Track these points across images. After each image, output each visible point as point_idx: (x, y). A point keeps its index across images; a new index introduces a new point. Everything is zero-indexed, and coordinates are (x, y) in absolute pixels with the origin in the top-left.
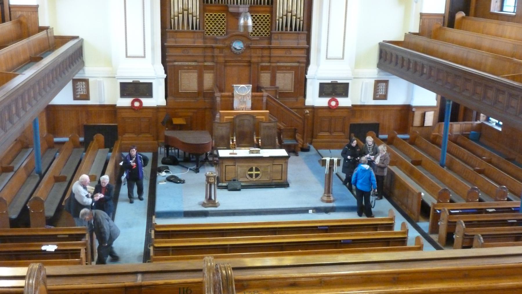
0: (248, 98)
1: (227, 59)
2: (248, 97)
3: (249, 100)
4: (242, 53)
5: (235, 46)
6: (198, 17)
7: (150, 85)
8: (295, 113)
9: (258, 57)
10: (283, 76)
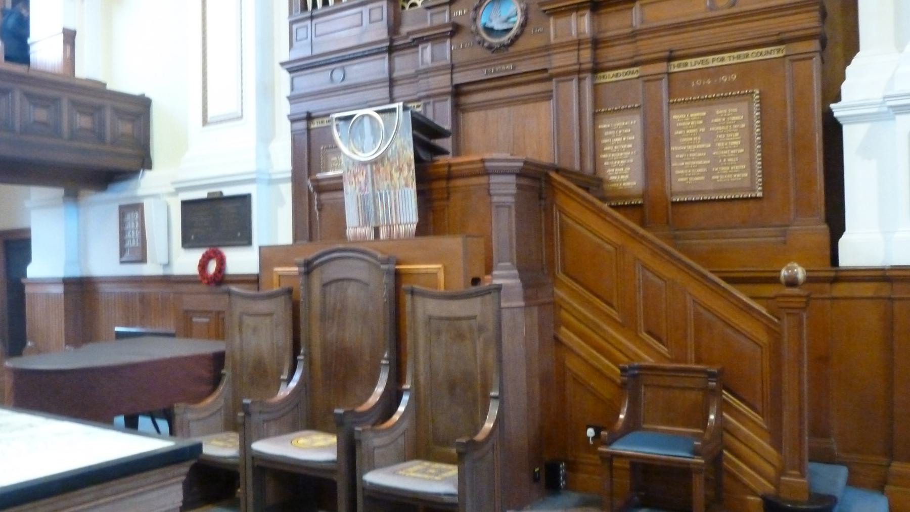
0: (396, 175)
1: (459, 78)
2: (400, 170)
3: (406, 189)
4: (513, 41)
5: (491, 21)
7: (244, 200)
8: (723, 284)
9: (579, 43)
10: (702, 118)
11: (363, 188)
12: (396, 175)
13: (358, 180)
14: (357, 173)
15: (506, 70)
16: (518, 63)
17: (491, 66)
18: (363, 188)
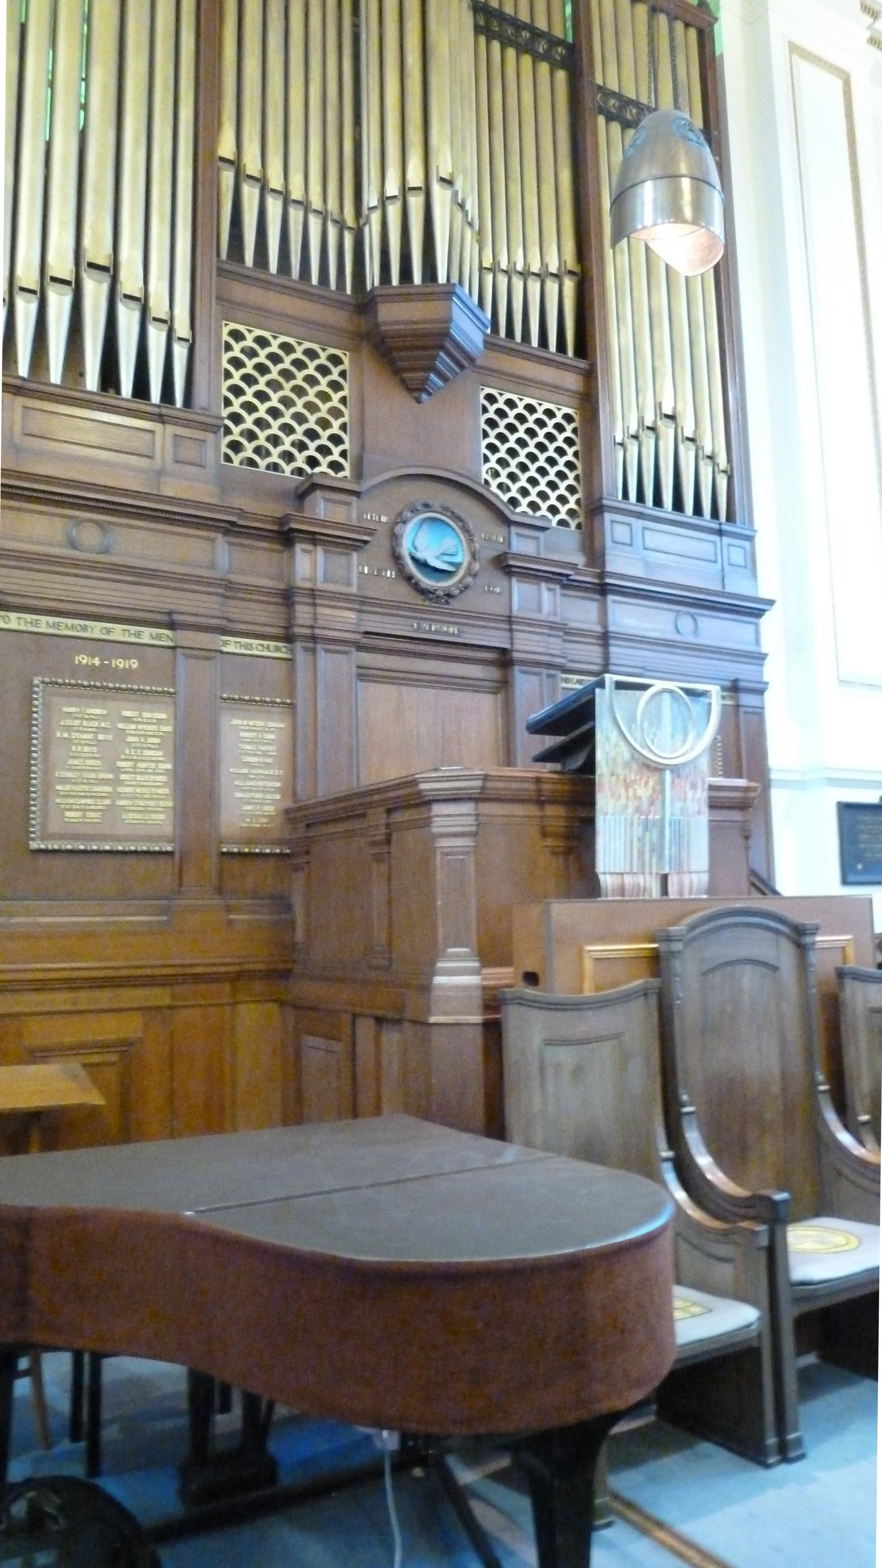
0: (690, 793)
2: (694, 786)
6: (182, 329)
11: (645, 806)
12: (690, 793)
13: (635, 791)
14: (634, 782)
15: (447, 633)
16: (465, 629)
17: (416, 618)
18: (645, 806)
